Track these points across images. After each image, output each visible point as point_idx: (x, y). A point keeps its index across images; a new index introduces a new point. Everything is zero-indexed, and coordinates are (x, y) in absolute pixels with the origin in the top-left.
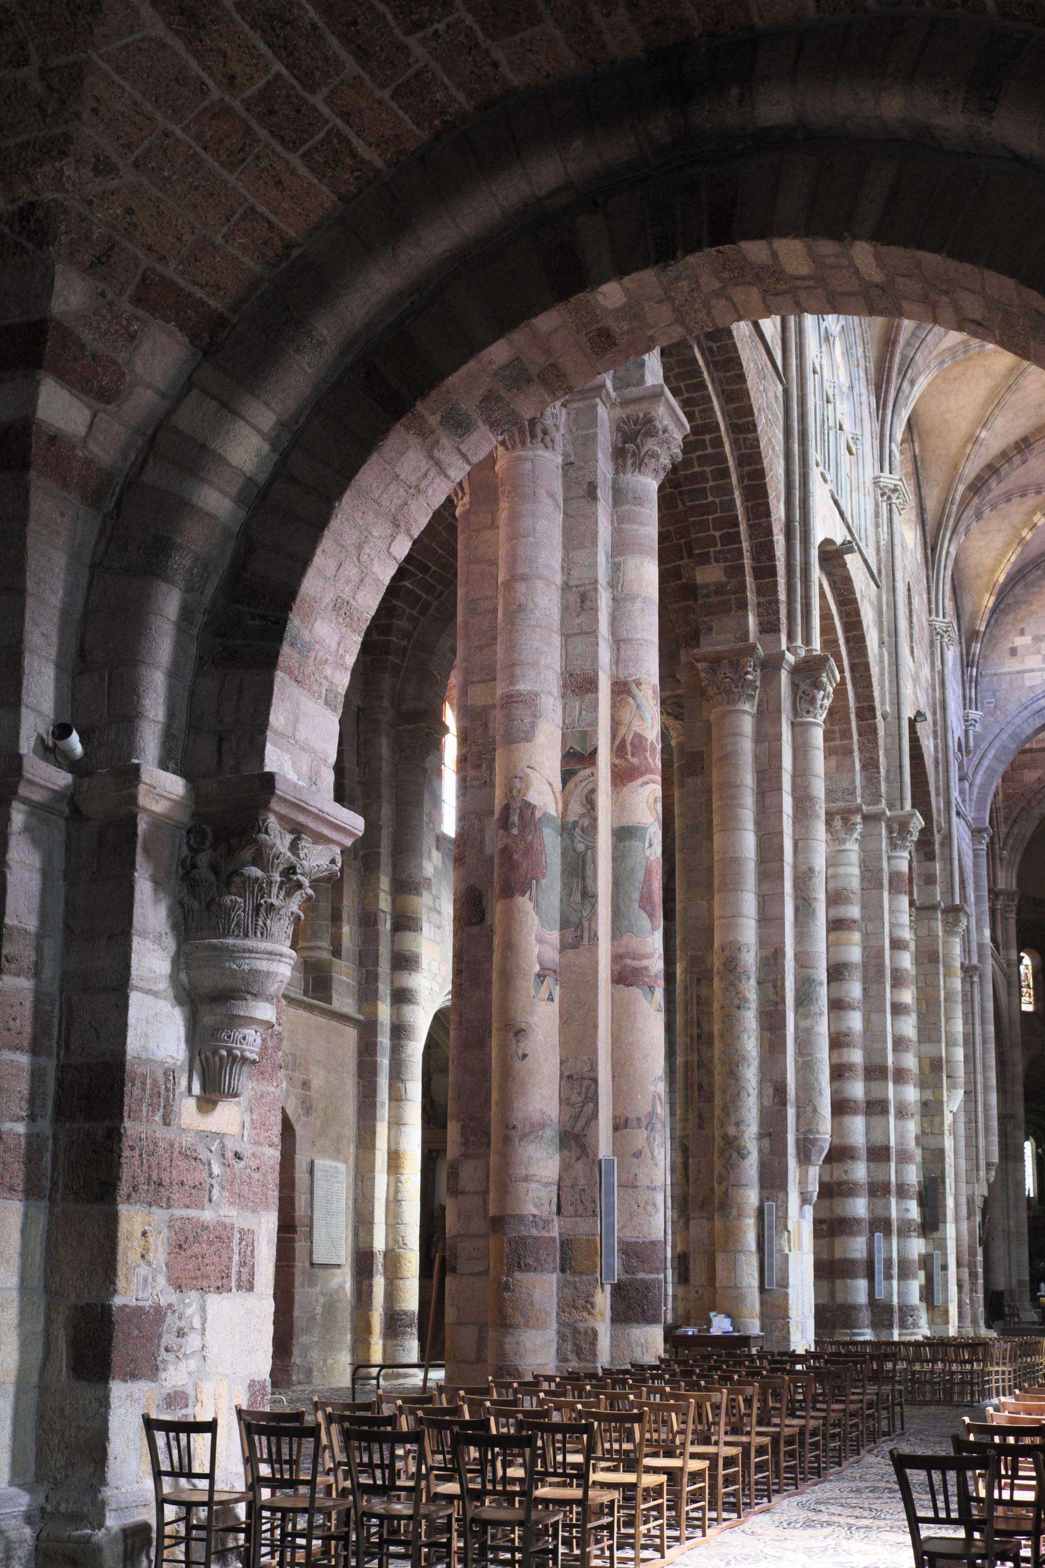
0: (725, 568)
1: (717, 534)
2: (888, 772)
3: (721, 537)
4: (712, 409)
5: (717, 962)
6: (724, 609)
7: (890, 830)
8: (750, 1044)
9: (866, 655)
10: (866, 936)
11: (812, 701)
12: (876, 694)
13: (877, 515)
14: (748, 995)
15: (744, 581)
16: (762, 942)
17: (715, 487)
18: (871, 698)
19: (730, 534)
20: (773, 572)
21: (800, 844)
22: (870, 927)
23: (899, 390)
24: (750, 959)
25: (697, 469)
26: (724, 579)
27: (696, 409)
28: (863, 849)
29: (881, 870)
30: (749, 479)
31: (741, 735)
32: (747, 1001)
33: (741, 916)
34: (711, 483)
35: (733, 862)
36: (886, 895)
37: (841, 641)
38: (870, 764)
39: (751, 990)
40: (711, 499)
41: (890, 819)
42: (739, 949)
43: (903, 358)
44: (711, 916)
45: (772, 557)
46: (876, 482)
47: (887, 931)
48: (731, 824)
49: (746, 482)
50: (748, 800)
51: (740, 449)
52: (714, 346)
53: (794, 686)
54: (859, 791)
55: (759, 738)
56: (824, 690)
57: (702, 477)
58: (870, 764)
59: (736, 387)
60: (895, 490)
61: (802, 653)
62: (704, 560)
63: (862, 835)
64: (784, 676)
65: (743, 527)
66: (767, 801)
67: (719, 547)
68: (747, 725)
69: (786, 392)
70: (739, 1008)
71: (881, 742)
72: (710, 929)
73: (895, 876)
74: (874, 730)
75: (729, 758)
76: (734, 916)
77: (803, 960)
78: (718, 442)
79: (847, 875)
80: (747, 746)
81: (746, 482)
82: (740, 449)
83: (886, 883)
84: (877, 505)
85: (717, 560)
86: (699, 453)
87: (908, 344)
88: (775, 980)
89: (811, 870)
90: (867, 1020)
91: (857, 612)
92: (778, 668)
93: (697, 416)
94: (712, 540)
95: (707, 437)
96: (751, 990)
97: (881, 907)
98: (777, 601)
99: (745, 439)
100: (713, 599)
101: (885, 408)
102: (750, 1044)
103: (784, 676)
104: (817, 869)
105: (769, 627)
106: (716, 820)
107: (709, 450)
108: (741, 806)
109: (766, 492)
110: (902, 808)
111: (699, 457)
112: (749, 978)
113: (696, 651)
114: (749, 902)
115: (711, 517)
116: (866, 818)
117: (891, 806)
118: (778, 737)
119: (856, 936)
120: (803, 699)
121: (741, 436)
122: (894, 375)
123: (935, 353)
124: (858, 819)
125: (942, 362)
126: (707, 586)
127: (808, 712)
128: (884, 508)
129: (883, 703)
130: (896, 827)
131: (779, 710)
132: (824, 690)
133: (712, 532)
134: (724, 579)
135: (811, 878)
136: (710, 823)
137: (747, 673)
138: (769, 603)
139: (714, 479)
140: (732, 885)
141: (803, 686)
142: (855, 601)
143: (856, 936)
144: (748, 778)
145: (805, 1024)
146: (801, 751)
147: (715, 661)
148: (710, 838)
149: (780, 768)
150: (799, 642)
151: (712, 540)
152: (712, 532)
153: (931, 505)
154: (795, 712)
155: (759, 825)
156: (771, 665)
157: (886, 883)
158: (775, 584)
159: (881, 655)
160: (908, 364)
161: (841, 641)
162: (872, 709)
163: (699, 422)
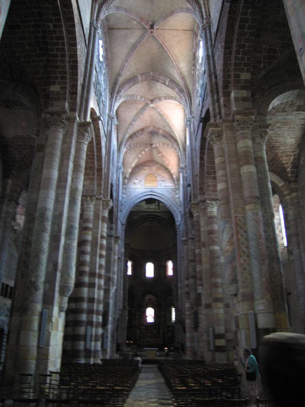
0: (60, 87)
1: (59, 76)
2: (104, 188)
3: (60, 77)
4: (62, 31)
5: (37, 214)
6: (58, 99)
7: (103, 204)
8: (46, 246)
9: (101, 153)
10: (93, 233)
11: (84, 136)
12: (103, 165)
13: (108, 123)
14: (47, 227)
15: (66, 92)
16: (55, 210)
17: (61, 60)
18: (101, 166)
19: (63, 76)
20: (76, 93)
21: (74, 180)
22: (95, 231)
23: (116, 97)
24: (50, 214)
25: (56, 53)
26: (60, 90)
27: (57, 30)
28: (95, 208)
29: (99, 214)
30: (73, 63)
31: (58, 138)
32: (46, 229)
33: (48, 198)
34: (60, 58)
35: (49, 179)
36: (100, 222)
37: (95, 147)
38: (99, 185)
39: (49, 225)
40: (59, 64)
41: (103, 201)
42: (46, 210)
43: (118, 90)
44: (37, 199)
45: (77, 89)
46: (109, 115)
47: (100, 232)
48: (50, 166)
49: (71, 64)
50: (57, 160)
51: (71, 52)
52: (66, 10)
53: (79, 130)
54: (95, 191)
55: (64, 142)
56: (88, 134)
57: (56, 55)
58: (99, 185)
59: (71, 29)
60: (113, 118)
61: (83, 121)
62: (54, 83)
63: (95, 204)
64: (76, 126)
65: (68, 75)
66: (64, 163)
67: (60, 80)
68: (61, 136)
69: (88, 53)
70: (43, 231)
71: (103, 179)
72: (36, 203)
73: (103, 217)
74: (101, 175)
75: (53, 145)
76: (46, 197)
77: (70, 219)
78: (63, 44)
79: (90, 214)
80: (59, 143)
81: (71, 64)
82: (71, 52)
83: (100, 218)
84: (108, 120)
85: (58, 84)
86: (57, 47)
87: (120, 87)
88: (58, 224)
89: (77, 188)
90: (91, 258)
91: (100, 140)
92: (74, 122)
93: (58, 33)
94: (57, 78)
95: (60, 41)
96: (49, 225)
97: (98, 225)
98: (76, 102)
99: (73, 49)
100: (55, 96)
101: (113, 99)
102: (46, 246)
103: (76, 126)
104: (79, 188)
105: (73, 110)
106: (45, 165)
107: (60, 47)
108: (54, 161)
109: (77, 67)
110: (107, 198)
111: (56, 49)
112: (48, 221)
113: (47, 110)
114: (52, 194)
115: (58, 70)
116: (97, 199)
117: (104, 197)
118: (71, 143)
119: (90, 233)
120: (81, 135)
121: (72, 48)
122: (116, 92)
123: (126, 94)
124: (94, 198)
125: (127, 97)
126: (54, 92)
127: (82, 139)
128: (110, 122)
129: (105, 169)
130: (105, 203)
131: (72, 134)
132: (88, 134)
133: (58, 75)
134: (60, 90)
135: (76, 191)
136: (42, 167)
137: (63, 119)
138: (74, 103)
139: (61, 57)
140: (48, 187)
141: (81, 131)
142: (100, 136)
143: (90, 233)
144: (58, 153)
145: (69, 242)
146: (78, 150)
147: (53, 114)
148: (42, 172)
149: (70, 152)
150: (82, 117)
151: (57, 78)
152: (58, 75)
153: (120, 138)
154: (78, 138)
155: (60, 170)
156: (71, 120)
157: (100, 218)
158: (76, 97)
159: (105, 157)
160: (119, 92)
161: (95, 147)
162: (102, 169)
163: (58, 35)
